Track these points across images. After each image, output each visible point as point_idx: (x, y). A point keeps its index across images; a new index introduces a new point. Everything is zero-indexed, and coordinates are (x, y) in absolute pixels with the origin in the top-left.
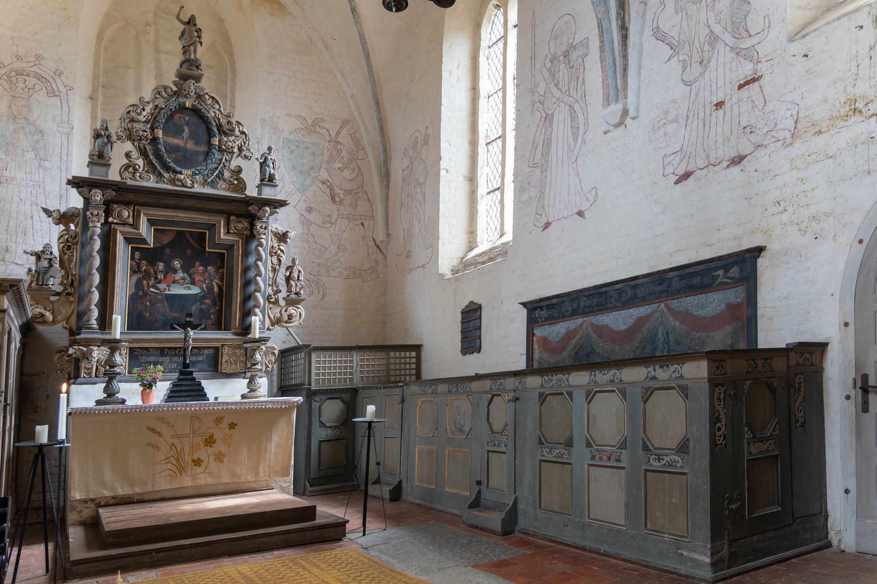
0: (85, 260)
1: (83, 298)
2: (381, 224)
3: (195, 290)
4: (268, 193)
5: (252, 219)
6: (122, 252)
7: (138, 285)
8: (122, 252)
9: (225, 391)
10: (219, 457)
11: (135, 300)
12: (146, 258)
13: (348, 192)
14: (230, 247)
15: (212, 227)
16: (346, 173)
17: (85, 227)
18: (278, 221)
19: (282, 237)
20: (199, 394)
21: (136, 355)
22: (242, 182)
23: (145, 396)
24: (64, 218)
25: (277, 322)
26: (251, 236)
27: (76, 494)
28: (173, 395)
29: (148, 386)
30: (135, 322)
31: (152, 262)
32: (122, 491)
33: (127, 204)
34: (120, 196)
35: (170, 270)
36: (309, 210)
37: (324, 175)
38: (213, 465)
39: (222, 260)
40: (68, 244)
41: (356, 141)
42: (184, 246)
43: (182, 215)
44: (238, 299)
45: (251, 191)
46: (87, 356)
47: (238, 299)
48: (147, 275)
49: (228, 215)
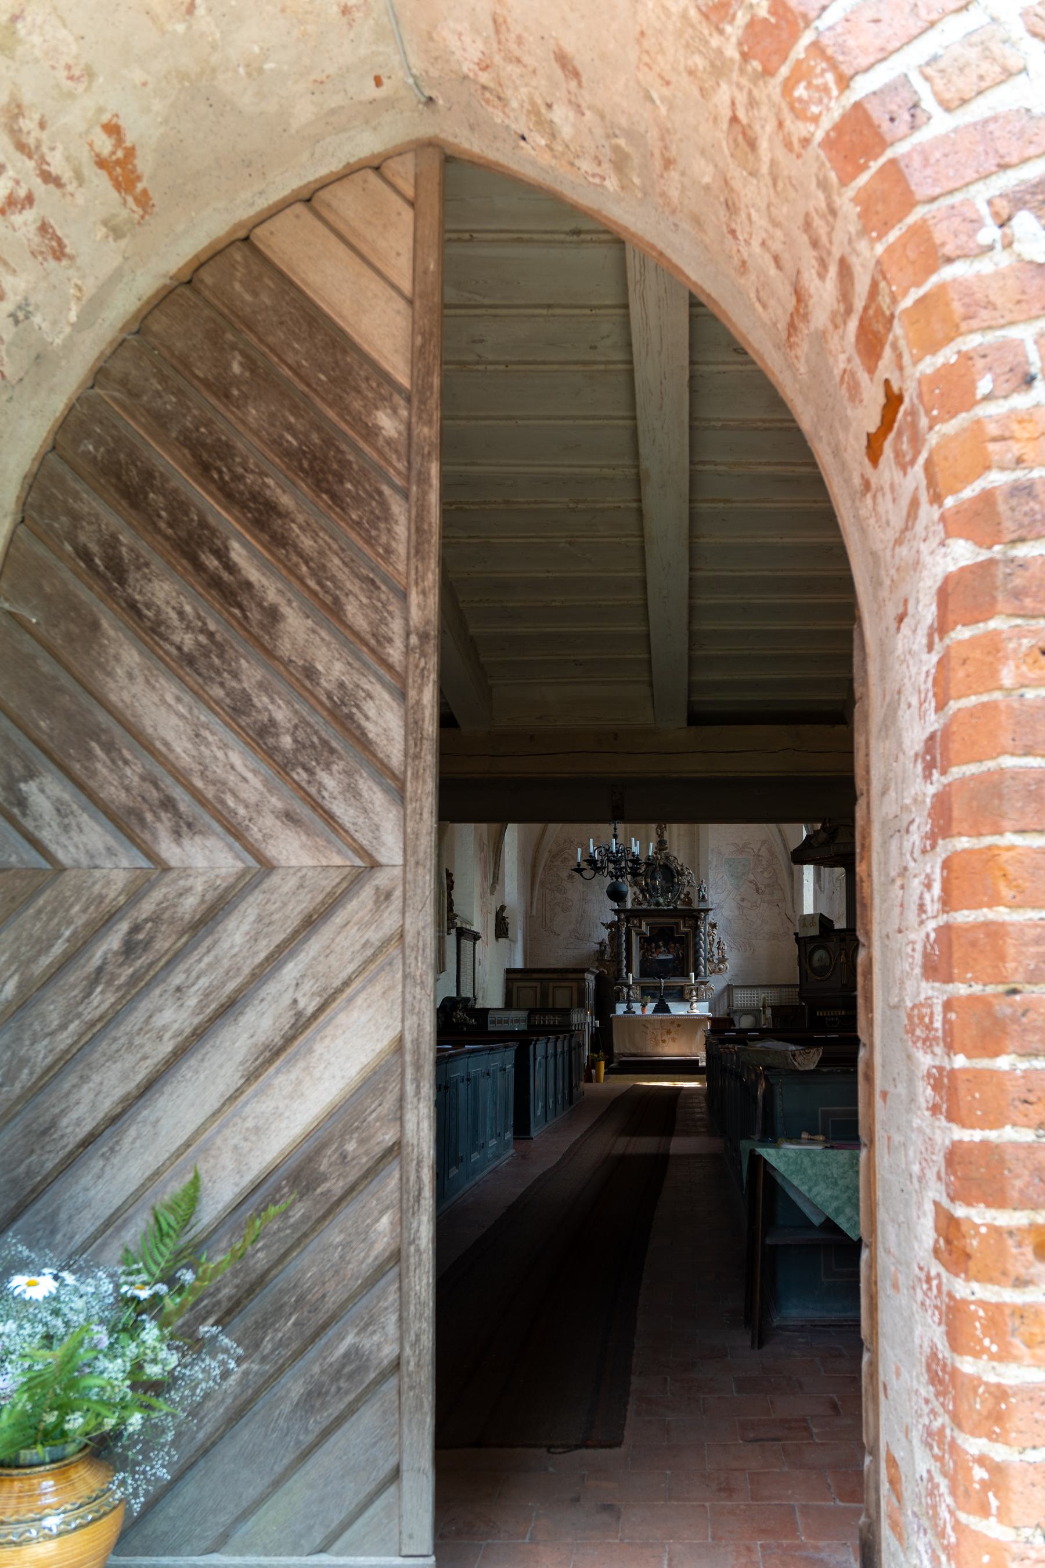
0: (620, 945)
1: (620, 962)
2: (790, 905)
3: (670, 957)
4: (702, 906)
5: (697, 919)
6: (635, 940)
7: (643, 956)
8: (635, 940)
9: (678, 1009)
10: (673, 1040)
11: (641, 962)
12: (647, 942)
13: (767, 886)
14: (687, 934)
15: (677, 925)
16: (766, 875)
17: (618, 929)
18: (711, 917)
19: (714, 926)
20: (667, 1010)
21: (645, 991)
22: (690, 900)
23: (643, 1011)
24: (609, 926)
25: (712, 972)
26: (696, 928)
27: (616, 1051)
28: (656, 1011)
29: (644, 1006)
30: (644, 973)
31: (649, 944)
32: (633, 1051)
33: (636, 917)
34: (633, 914)
35: (658, 947)
36: (743, 900)
37: (751, 877)
38: (671, 1043)
39: (683, 941)
40: (614, 937)
41: (772, 854)
42: (663, 936)
43: (661, 920)
44: (691, 960)
45: (696, 905)
46: (621, 990)
47: (691, 960)
48: (647, 950)
49: (684, 917)
